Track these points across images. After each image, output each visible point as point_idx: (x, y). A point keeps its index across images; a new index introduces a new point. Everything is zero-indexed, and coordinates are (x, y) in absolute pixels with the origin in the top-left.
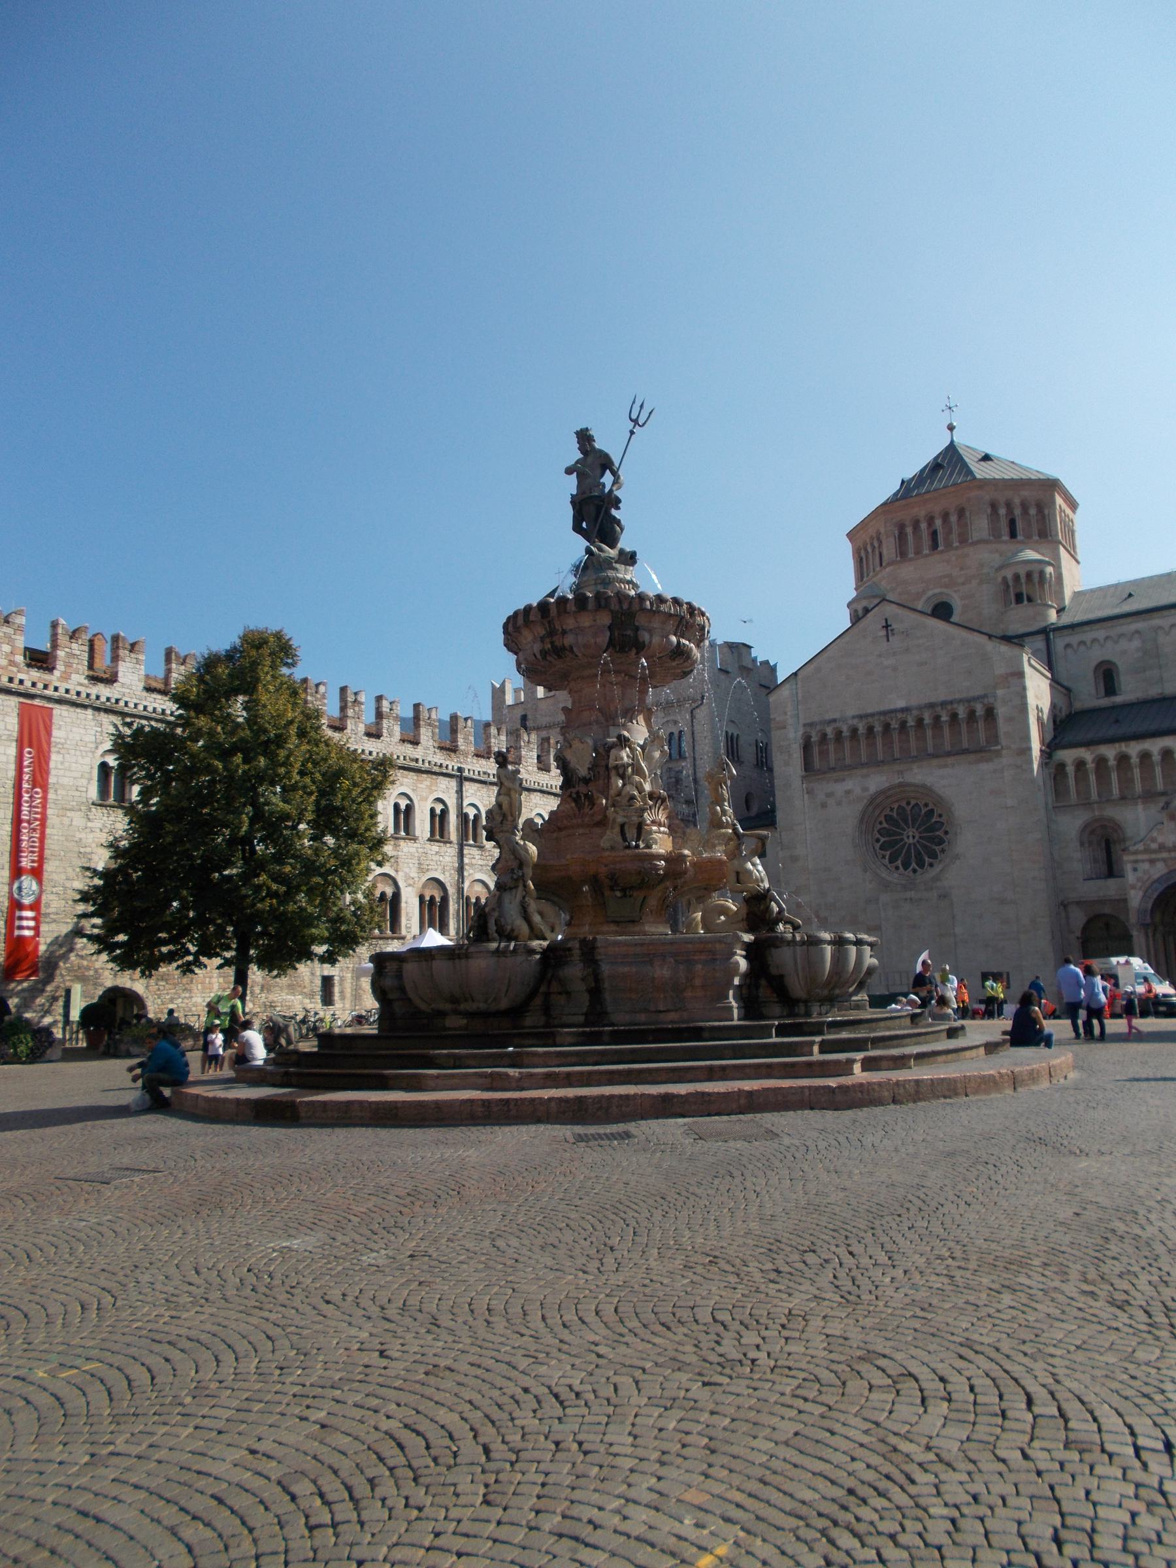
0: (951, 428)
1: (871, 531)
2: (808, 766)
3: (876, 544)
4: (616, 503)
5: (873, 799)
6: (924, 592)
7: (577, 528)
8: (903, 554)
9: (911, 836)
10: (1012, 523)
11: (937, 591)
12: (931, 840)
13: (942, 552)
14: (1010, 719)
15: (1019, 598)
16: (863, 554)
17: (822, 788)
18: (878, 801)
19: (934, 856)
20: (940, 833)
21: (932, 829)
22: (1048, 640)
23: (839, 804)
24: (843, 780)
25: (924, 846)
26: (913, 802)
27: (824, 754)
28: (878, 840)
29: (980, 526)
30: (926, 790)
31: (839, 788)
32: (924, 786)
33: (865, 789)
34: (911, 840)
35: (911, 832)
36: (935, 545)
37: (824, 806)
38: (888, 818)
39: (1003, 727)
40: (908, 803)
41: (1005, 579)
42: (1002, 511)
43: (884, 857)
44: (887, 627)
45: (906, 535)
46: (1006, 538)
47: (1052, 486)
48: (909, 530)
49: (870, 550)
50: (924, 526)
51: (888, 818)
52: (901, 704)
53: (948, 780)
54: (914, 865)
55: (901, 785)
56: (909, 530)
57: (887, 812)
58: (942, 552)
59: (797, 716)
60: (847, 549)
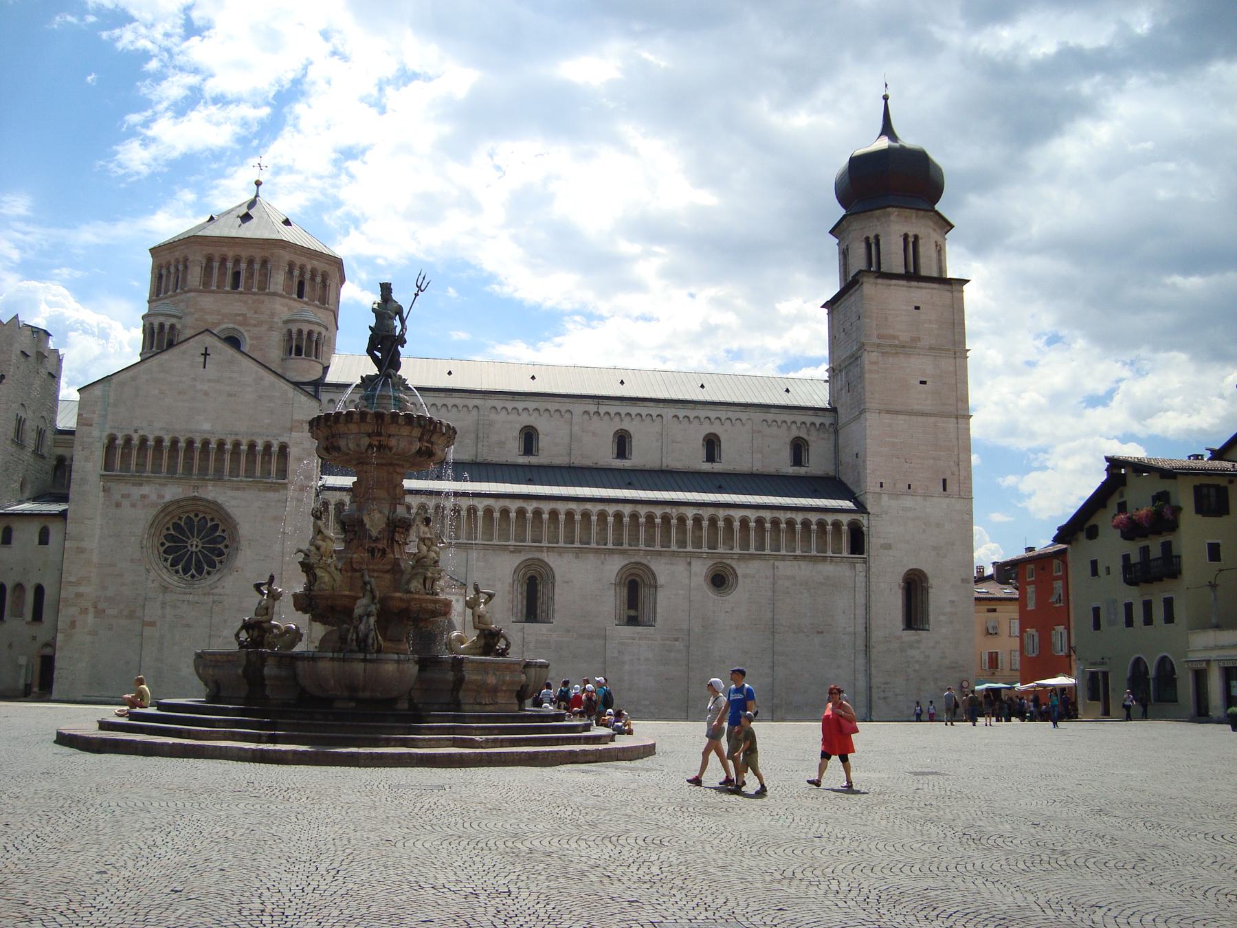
0: (258, 183)
1: (178, 254)
2: (108, 465)
3: (181, 267)
4: (402, 341)
5: (167, 506)
6: (219, 324)
7: (370, 351)
8: (206, 283)
9: (195, 544)
10: (301, 285)
11: (231, 326)
12: (212, 550)
13: (241, 293)
15: (299, 352)
16: (164, 272)
17: (119, 489)
18: (170, 509)
19: (212, 564)
21: (214, 541)
22: (317, 392)
23: (133, 506)
24: (141, 485)
25: (205, 556)
26: (201, 516)
27: (126, 457)
28: (163, 544)
29: (278, 281)
30: (216, 506)
31: (136, 492)
32: (215, 503)
33: (161, 496)
34: (194, 549)
36: (235, 285)
37: (118, 505)
38: (177, 526)
39: (292, 465)
40: (196, 515)
41: (290, 332)
42: (296, 272)
43: (166, 560)
44: (206, 355)
45: (212, 268)
46: (295, 296)
47: (337, 263)
48: (216, 265)
49: (172, 270)
50: (230, 265)
51: (177, 526)
52: (207, 426)
53: (238, 501)
54: (193, 571)
55: (194, 498)
56: (216, 265)
57: (176, 520)
58: (241, 293)
59: (105, 416)
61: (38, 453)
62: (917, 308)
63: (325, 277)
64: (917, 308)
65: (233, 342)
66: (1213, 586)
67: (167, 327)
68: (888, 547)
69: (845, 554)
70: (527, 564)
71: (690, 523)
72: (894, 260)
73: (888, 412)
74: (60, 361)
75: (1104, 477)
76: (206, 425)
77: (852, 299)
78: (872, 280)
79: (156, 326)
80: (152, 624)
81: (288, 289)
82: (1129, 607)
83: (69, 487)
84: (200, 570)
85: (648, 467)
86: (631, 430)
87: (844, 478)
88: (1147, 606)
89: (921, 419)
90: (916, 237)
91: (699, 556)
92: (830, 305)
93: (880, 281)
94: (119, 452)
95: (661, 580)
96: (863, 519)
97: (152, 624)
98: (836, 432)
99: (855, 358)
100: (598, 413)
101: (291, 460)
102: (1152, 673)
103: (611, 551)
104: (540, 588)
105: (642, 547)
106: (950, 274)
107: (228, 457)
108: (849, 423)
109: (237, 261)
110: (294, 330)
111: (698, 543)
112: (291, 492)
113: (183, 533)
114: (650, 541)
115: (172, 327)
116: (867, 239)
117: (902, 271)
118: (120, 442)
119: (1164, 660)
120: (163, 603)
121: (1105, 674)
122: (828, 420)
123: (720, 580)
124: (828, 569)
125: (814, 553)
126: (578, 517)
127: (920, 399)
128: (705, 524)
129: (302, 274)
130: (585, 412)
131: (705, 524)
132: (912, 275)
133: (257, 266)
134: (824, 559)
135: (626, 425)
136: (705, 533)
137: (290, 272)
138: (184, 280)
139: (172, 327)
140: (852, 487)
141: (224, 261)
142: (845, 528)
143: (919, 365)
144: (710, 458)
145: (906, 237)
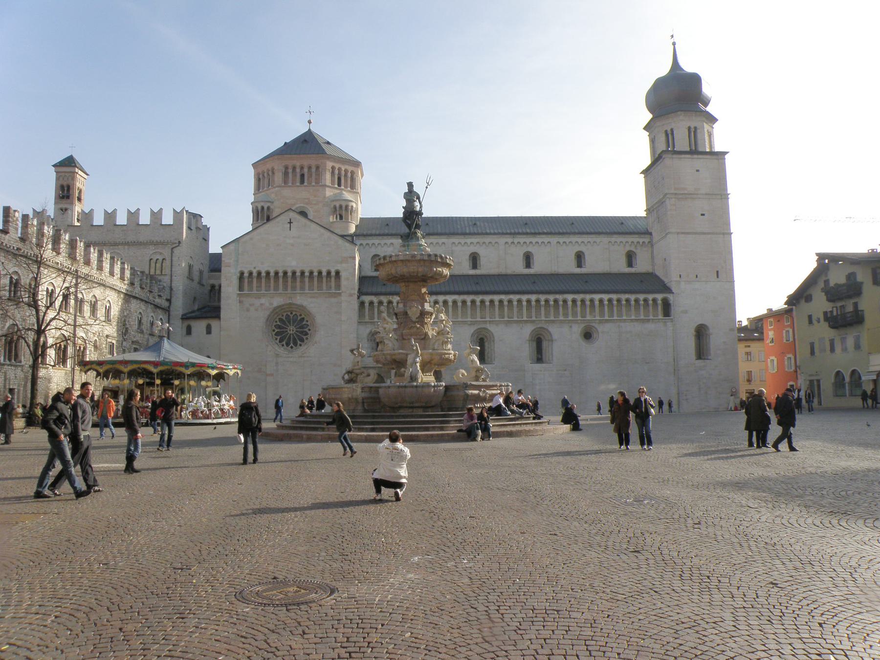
0: (310, 122)
1: (269, 166)
2: (241, 288)
3: (270, 173)
5: (275, 309)
6: (294, 204)
8: (285, 182)
9: (291, 330)
10: (339, 179)
12: (302, 332)
14: (348, 279)
16: (261, 176)
19: (302, 340)
20: (306, 330)
21: (302, 327)
23: (256, 310)
27: (250, 283)
31: (257, 302)
33: (271, 304)
35: (292, 328)
36: (302, 182)
37: (248, 310)
38: (281, 320)
39: (344, 282)
41: (335, 207)
42: (337, 172)
44: (290, 223)
48: (290, 171)
50: (298, 170)
51: (281, 320)
52: (294, 263)
56: (290, 171)
59: (237, 261)
60: (251, 172)
61: (200, 283)
62: (698, 171)
63: (353, 173)
64: (698, 171)
65: (303, 214)
67: (265, 208)
68: (686, 312)
69: (660, 317)
70: (478, 331)
71: (570, 303)
72: (682, 144)
73: (683, 233)
74: (208, 229)
75: (815, 265)
76: (292, 264)
77: (659, 166)
78: (670, 156)
79: (259, 208)
80: (272, 375)
81: (333, 182)
83: (219, 300)
84: (295, 344)
86: (533, 252)
87: (657, 274)
90: (695, 128)
91: (575, 322)
92: (646, 172)
93: (675, 156)
94: (246, 280)
95: (555, 336)
96: (670, 297)
97: (272, 375)
98: (652, 246)
99: (661, 203)
100: (513, 243)
101: (343, 279)
102: (847, 379)
103: (526, 322)
104: (486, 344)
105: (543, 318)
106: (717, 149)
107: (307, 280)
108: (659, 241)
109: (302, 168)
110: (338, 206)
111: (575, 314)
112: (344, 298)
113: (285, 324)
114: (547, 315)
115: (268, 208)
116: (666, 131)
117: (688, 149)
118: (246, 275)
120: (277, 364)
121: (818, 381)
122: (647, 240)
123: (588, 335)
124: (651, 326)
125: (642, 317)
126: (506, 303)
128: (579, 303)
129: (339, 174)
130: (506, 243)
131: (579, 303)
132: (694, 151)
133: (314, 170)
134: (648, 320)
135: (530, 249)
136: (579, 309)
137: (333, 173)
138: (273, 181)
139: (268, 208)
140: (663, 278)
141: (294, 168)
142: (660, 302)
144: (579, 265)
145: (689, 128)
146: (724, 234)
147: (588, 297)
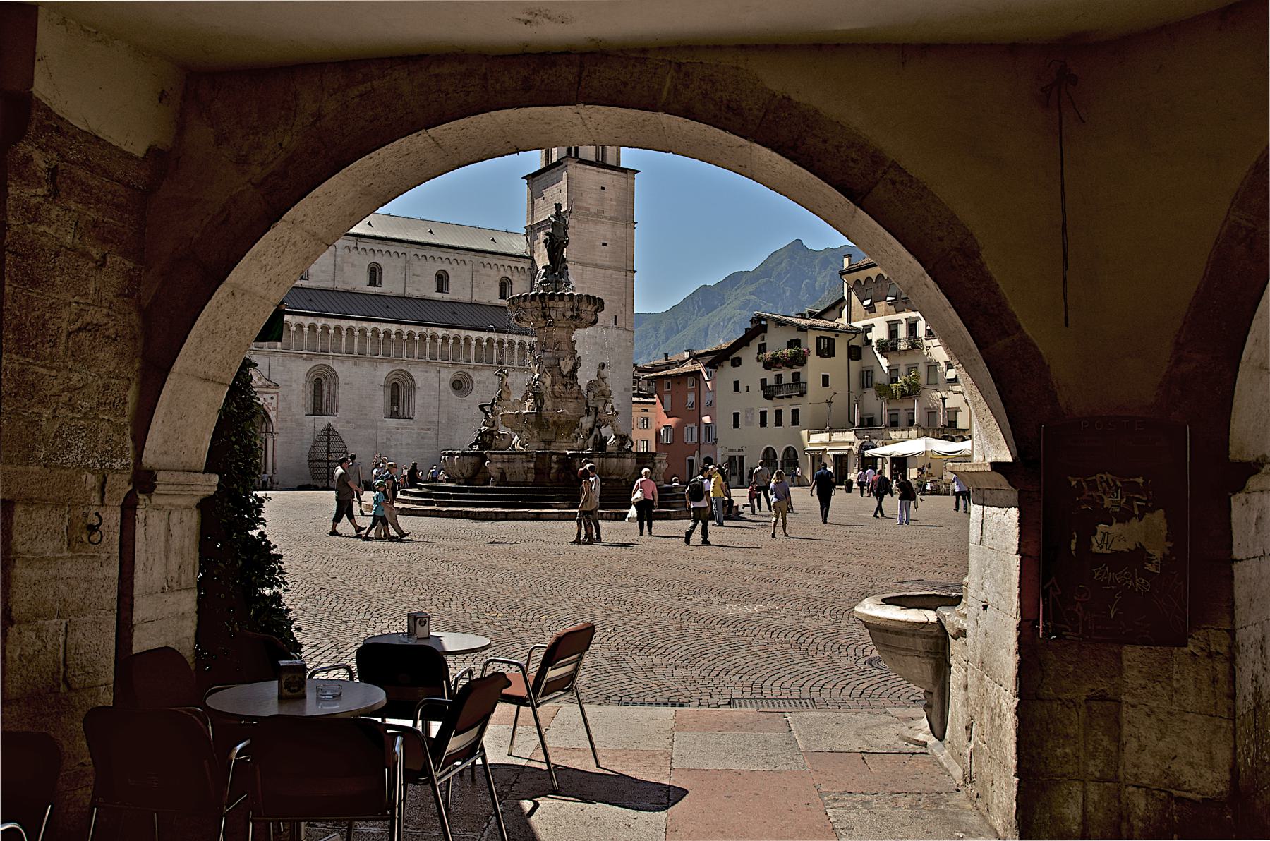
66: (829, 403)
73: (580, 264)
82: (763, 414)
85: (395, 293)
88: (779, 414)
89: (602, 271)
92: (530, 178)
95: (418, 384)
102: (779, 457)
106: (622, 166)
119: (788, 449)
121: (742, 458)
123: (460, 385)
127: (602, 256)
130: (348, 247)
132: (600, 164)
135: (378, 259)
143: (603, 230)
144: (440, 290)
146: (626, 271)
147: (463, 333)
